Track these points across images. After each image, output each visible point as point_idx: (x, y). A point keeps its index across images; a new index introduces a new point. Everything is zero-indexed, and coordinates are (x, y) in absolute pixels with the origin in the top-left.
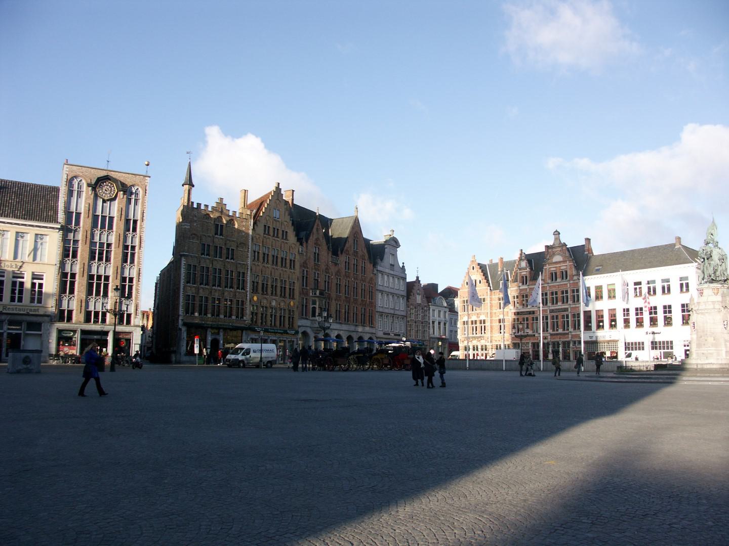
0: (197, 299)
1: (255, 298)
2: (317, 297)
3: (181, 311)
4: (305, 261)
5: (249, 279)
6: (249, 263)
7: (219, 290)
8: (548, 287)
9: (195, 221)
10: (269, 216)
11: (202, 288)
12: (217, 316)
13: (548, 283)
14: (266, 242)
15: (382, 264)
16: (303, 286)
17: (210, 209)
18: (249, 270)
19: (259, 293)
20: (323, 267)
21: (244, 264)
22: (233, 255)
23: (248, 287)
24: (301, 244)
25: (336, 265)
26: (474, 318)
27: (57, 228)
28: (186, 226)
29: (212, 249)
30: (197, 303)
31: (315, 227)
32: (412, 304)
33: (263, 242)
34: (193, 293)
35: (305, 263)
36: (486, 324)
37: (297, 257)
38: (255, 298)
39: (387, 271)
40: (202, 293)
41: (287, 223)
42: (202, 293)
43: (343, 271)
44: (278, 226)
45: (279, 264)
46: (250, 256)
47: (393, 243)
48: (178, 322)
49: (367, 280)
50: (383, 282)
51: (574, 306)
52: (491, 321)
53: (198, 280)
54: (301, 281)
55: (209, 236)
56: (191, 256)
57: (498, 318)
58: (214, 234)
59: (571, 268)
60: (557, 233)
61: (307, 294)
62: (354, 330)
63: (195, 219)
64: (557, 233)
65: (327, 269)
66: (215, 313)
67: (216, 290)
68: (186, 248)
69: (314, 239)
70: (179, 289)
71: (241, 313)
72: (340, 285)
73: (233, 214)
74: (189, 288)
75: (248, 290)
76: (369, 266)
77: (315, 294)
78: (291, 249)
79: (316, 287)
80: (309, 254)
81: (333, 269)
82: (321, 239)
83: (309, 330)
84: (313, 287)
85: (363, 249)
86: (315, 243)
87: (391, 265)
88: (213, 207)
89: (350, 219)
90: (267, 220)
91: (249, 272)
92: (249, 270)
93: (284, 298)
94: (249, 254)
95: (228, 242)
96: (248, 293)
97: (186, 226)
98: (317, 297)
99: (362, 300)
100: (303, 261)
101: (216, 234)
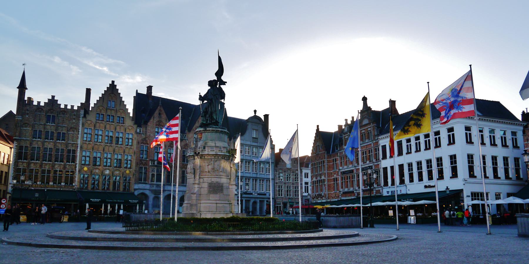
2: (156, 166)
7: (50, 164)
9: (28, 114)
24: (139, 126)
26: (319, 178)
31: (157, 112)
32: (281, 169)
37: (135, 136)
38: (86, 169)
39: (249, 143)
40: (32, 166)
42: (32, 166)
44: (113, 113)
45: (114, 142)
46: (80, 137)
51: (376, 164)
55: (41, 124)
59: (373, 129)
60: (365, 99)
67: (46, 164)
68: (17, 134)
69: (155, 122)
75: (78, 162)
77: (154, 164)
80: (148, 134)
83: (147, 192)
86: (156, 125)
91: (79, 149)
94: (80, 136)
96: (77, 165)
98: (156, 166)
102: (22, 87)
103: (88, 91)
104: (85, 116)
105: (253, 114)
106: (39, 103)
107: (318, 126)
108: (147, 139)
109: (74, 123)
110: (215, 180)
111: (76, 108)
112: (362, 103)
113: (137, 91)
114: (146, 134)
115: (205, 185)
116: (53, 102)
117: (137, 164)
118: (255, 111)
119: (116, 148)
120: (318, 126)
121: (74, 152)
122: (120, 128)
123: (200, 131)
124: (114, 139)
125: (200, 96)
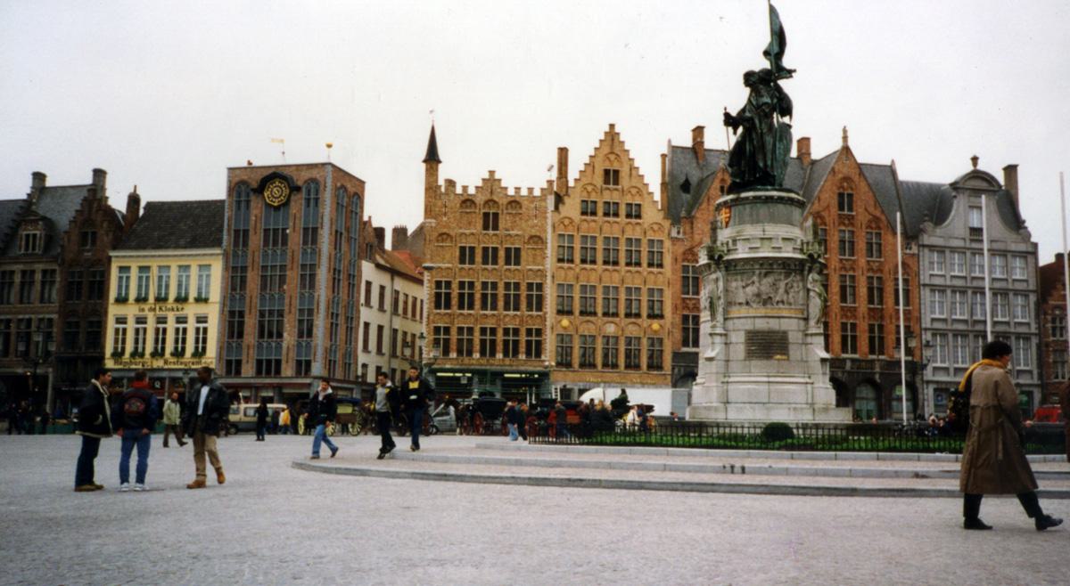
0: (454, 332)
5: (550, 294)
9: (445, 214)
10: (591, 184)
15: (938, 231)
17: (472, 191)
21: (539, 270)
27: (218, 255)
37: (667, 244)
71: (535, 349)
73: (516, 192)
85: (871, 209)
96: (548, 316)
102: (432, 158)
103: (563, 153)
104: (557, 208)
105: (969, 168)
106: (465, 188)
110: (761, 325)
111: (537, 193)
113: (669, 141)
114: (692, 238)
115: (738, 338)
116: (491, 182)
117: (675, 308)
118: (975, 160)
119: (628, 274)
121: (540, 287)
122: (633, 230)
123: (725, 203)
125: (727, 115)
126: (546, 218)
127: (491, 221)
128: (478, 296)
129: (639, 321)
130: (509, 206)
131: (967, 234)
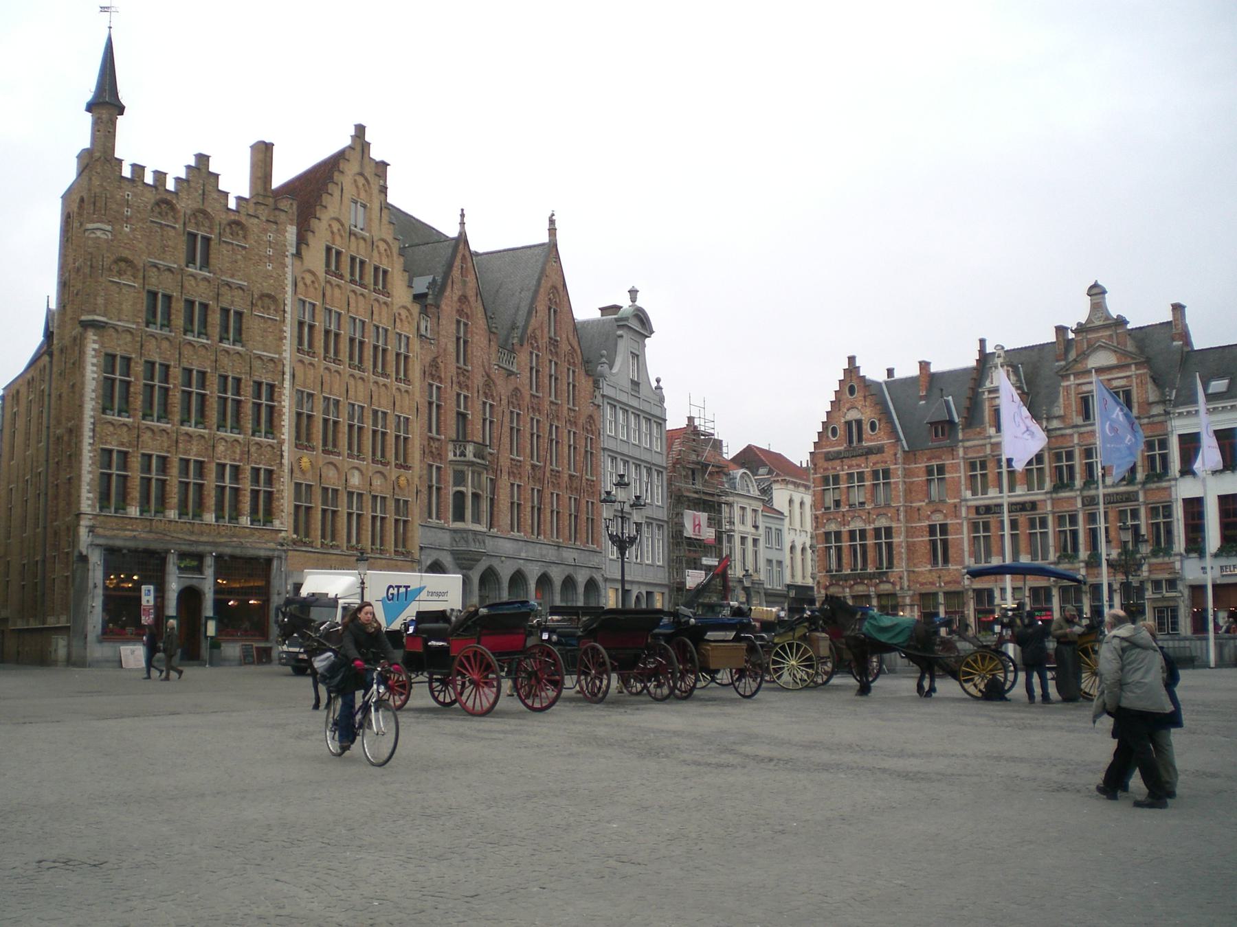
0: (136, 462)
1: (305, 462)
3: (87, 500)
4: (434, 359)
6: (287, 355)
7: (202, 437)
8: (1076, 436)
10: (338, 220)
11: (148, 428)
12: (194, 516)
13: (1077, 426)
14: (332, 295)
16: (430, 430)
17: (170, 185)
18: (287, 377)
19: (313, 449)
20: (478, 380)
21: (272, 360)
22: (239, 331)
23: (285, 430)
24: (424, 311)
25: (509, 375)
26: (857, 525)
28: (99, 233)
29: (178, 307)
30: (135, 474)
31: (458, 262)
33: (324, 295)
34: (122, 444)
35: (434, 364)
36: (895, 540)
37: (416, 345)
38: (305, 462)
41: (385, 246)
43: (526, 392)
44: (361, 252)
45: (368, 363)
47: (635, 324)
48: (76, 535)
49: (582, 420)
50: (616, 430)
52: (910, 532)
53: (138, 402)
54: (426, 417)
55: (169, 270)
56: (114, 328)
57: (927, 523)
58: (183, 264)
59: (1142, 384)
60: (1096, 292)
61: (440, 456)
62: (554, 559)
63: (128, 212)
64: (1096, 292)
65: (487, 385)
66: (192, 503)
68: (100, 301)
69: (455, 298)
70: (75, 432)
71: (265, 507)
72: (518, 430)
74: (111, 429)
76: (585, 383)
77: (463, 454)
78: (398, 323)
79: (461, 439)
80: (443, 340)
81: (503, 388)
82: (472, 299)
84: (454, 437)
85: (571, 337)
87: (633, 381)
88: (178, 180)
89: (537, 251)
90: (332, 233)
91: (287, 384)
92: (287, 377)
93: (382, 463)
95: (224, 290)
96: (285, 448)
97: (99, 233)
98: (472, 464)
99: (571, 476)
100: (428, 359)
101: (191, 260)
102: (106, 104)
103: (263, 154)
104: (298, 255)
106: (160, 176)
107: (852, 359)
108: (439, 360)
109: (268, 276)
112: (1086, 302)
118: (633, 293)
120: (852, 359)
124: (368, 353)
126: (284, 266)
127: (199, 249)
128: (176, 398)
129: (386, 470)
130: (228, 230)
131: (628, 386)
